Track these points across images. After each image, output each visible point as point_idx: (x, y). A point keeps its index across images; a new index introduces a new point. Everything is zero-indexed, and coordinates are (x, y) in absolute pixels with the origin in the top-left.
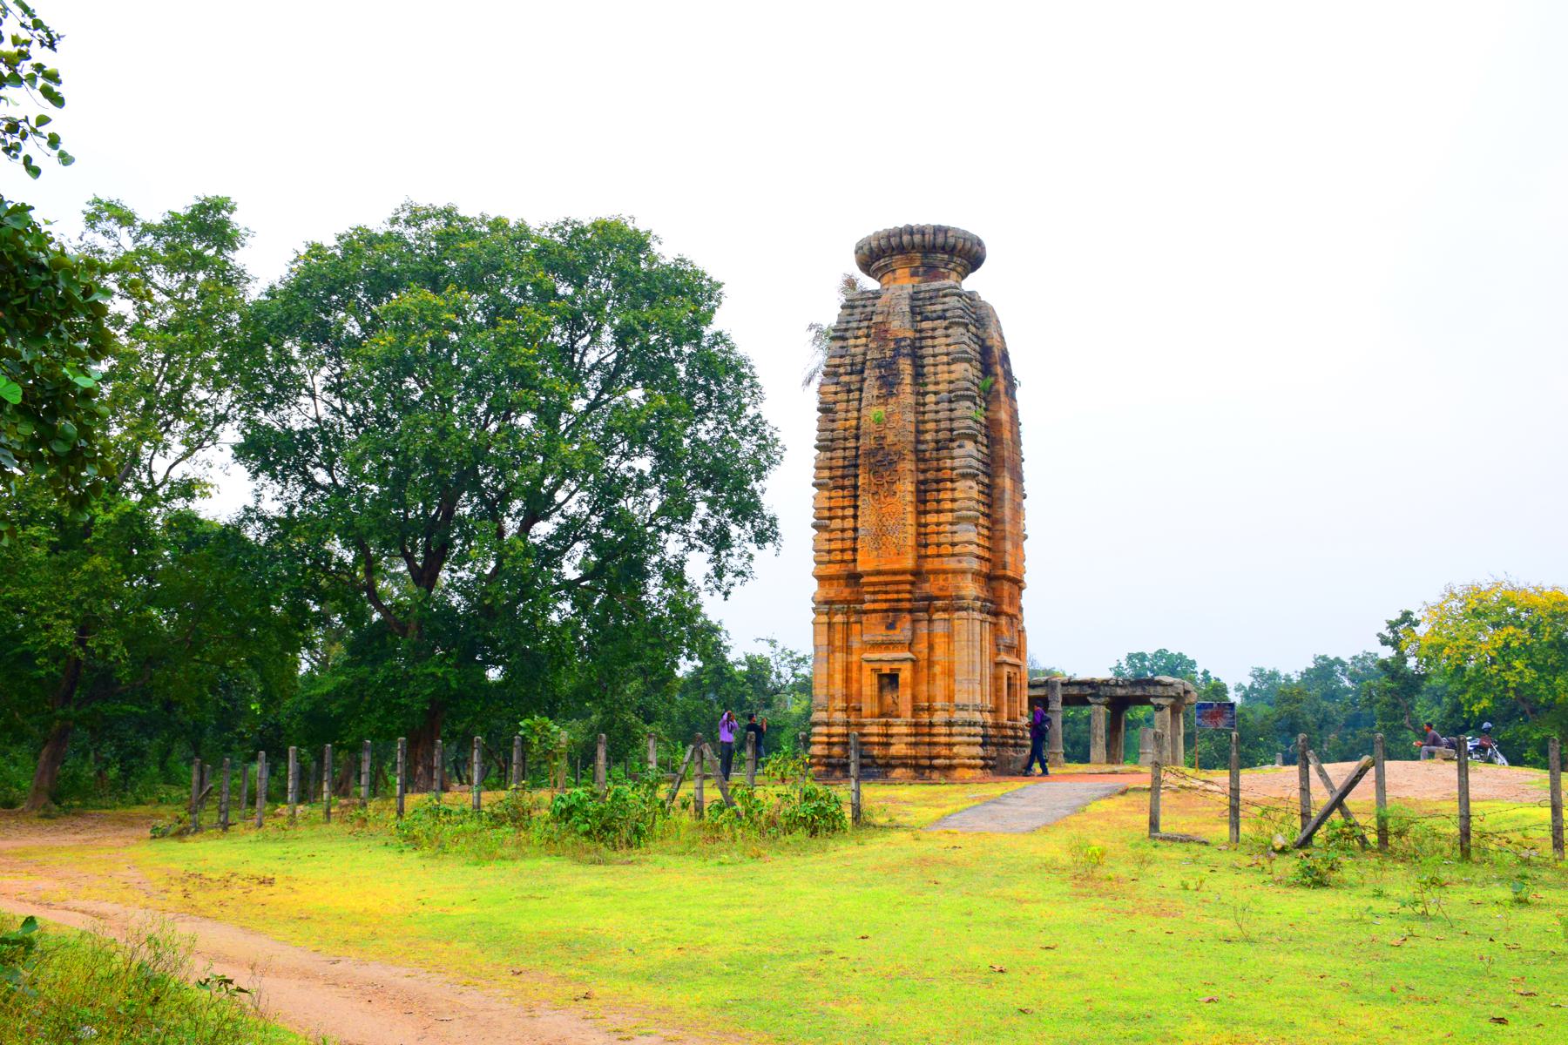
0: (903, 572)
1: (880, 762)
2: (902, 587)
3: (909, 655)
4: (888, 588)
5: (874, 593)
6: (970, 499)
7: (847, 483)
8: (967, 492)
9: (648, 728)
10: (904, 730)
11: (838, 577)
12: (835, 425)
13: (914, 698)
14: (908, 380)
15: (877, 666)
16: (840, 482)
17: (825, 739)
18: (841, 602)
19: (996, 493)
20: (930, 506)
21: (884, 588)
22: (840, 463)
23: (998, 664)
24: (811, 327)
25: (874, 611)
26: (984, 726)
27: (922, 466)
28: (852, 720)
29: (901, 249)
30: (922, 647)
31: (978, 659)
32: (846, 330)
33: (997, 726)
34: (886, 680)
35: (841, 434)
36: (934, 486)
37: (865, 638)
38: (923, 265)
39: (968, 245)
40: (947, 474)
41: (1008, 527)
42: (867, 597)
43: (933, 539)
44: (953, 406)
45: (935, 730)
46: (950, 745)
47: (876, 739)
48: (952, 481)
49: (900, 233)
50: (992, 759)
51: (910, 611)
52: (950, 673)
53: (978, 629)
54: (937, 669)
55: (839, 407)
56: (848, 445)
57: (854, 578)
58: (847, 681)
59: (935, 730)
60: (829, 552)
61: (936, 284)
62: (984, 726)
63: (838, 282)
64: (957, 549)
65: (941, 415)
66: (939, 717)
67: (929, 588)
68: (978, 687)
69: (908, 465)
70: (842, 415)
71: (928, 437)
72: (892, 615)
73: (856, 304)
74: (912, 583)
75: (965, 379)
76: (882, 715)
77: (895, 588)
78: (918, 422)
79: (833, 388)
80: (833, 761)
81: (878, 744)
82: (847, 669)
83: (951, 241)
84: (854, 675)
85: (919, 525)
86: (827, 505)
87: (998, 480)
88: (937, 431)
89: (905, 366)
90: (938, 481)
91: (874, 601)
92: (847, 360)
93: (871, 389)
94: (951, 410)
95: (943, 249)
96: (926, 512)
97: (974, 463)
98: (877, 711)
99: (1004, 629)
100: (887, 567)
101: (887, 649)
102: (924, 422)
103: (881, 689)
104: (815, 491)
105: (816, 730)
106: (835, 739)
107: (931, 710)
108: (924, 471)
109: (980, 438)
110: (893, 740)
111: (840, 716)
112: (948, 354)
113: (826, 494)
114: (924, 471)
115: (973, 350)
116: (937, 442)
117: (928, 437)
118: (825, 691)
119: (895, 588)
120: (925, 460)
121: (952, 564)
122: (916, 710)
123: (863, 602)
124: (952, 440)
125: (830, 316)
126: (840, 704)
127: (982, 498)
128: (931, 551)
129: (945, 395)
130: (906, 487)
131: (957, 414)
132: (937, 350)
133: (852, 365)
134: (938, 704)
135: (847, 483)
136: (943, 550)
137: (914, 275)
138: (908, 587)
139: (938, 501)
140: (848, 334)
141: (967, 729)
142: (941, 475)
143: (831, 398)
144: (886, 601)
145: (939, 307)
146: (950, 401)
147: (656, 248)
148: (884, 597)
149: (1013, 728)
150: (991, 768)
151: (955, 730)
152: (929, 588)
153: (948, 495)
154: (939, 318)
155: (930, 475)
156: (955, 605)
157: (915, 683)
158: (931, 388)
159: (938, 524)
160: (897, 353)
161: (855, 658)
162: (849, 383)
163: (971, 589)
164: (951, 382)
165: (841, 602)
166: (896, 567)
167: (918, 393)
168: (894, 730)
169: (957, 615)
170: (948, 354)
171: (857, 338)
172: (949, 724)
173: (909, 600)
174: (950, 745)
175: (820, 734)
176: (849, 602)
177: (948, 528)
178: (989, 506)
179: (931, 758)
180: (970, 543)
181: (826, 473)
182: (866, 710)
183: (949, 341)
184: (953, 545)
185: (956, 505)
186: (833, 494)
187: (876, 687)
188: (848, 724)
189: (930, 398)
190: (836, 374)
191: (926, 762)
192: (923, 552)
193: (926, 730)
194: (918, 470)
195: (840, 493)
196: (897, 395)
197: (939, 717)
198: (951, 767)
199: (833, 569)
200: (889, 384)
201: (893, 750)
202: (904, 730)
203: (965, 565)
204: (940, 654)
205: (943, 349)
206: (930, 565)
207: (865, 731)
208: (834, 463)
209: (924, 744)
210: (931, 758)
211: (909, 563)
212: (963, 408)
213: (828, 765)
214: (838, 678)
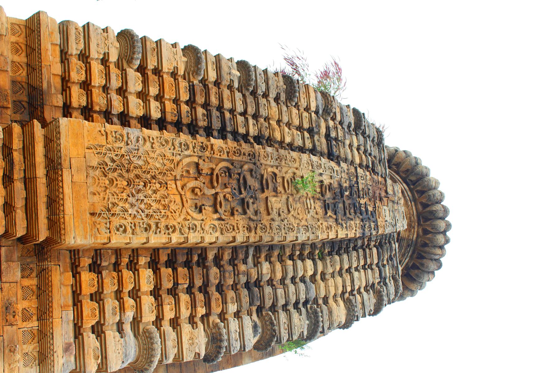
4: (19, 186)
20: (166, 272)
21: (18, 174)
22: (227, 105)
36: (198, 282)
40: (216, 309)
60: (84, 57)
64: (91, 340)
71: (266, 267)
77: (19, 203)
85: (135, 253)
89: (350, 230)
96: (154, 265)
100: (67, 189)
114: (217, 260)
117: (266, 267)
119: (19, 203)
120: (232, 262)
124: (259, 310)
128: (87, 278)
130: (207, 232)
131: (295, 315)
133: (336, 139)
136: (88, 307)
139: (173, 292)
159: (135, 294)
166: (69, 206)
177: (130, 314)
181: (212, 76)
184: (98, 330)
185: (166, 327)
186: (183, 84)
192: (86, 261)
195: (185, 97)
206: (61, 281)
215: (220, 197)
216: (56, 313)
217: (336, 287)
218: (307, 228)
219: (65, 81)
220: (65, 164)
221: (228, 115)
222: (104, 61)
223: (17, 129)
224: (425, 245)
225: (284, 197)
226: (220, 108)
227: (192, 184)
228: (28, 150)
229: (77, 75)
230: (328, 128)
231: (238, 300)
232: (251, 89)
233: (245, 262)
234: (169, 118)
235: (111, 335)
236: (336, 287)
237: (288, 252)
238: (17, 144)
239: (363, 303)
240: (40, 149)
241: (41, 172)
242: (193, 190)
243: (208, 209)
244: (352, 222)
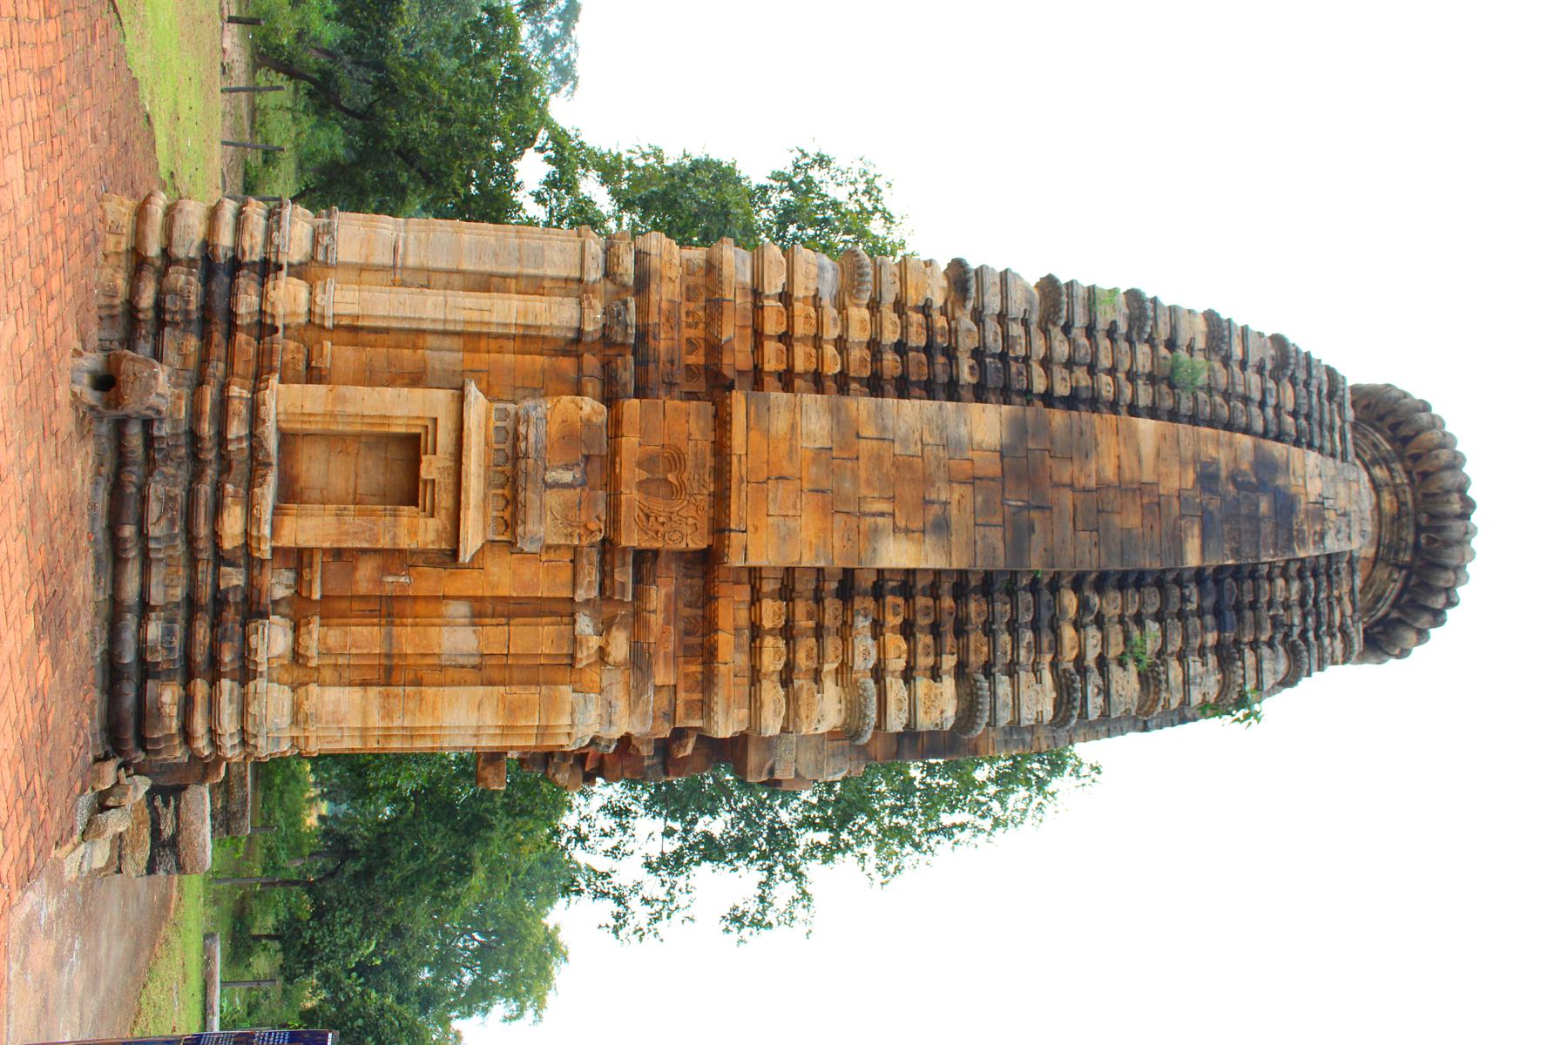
62: (267, 269)
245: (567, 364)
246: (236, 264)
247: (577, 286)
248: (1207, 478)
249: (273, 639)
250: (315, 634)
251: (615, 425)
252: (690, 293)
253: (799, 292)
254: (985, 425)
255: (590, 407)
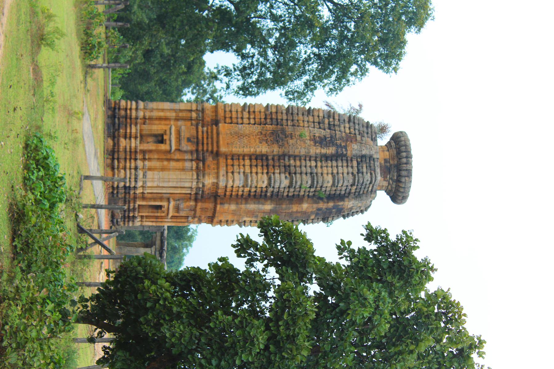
0: (218, 146)
1: (116, 133)
2: (210, 146)
3: (174, 148)
4: (210, 140)
5: (207, 132)
6: (257, 182)
7: (268, 121)
8: (261, 181)
9: (139, 53)
10: (133, 145)
11: (216, 116)
12: (300, 116)
13: (150, 151)
14: (324, 151)
15: (168, 132)
16: (269, 117)
17: (129, 107)
18: (203, 116)
19: (262, 201)
22: (279, 117)
23: (168, 200)
24: (360, 106)
25: (197, 132)
26: (135, 188)
27: (276, 158)
28: (139, 121)
29: (399, 152)
30: (178, 156)
31: (171, 184)
32: (354, 123)
33: (135, 198)
34: (160, 138)
35: (296, 118)
36: (265, 164)
37: (183, 128)
38: (391, 165)
39: (402, 190)
40: (271, 170)
41: (243, 206)
42: (205, 129)
43: (236, 163)
44: (309, 175)
45: (133, 161)
46: (125, 169)
47: (128, 131)
48: (267, 173)
49: (408, 151)
50: (117, 192)
51: (197, 151)
52: (163, 169)
53: (187, 185)
54: (166, 163)
55: (311, 119)
56: (289, 122)
57: (216, 122)
58: (160, 119)
59: (133, 161)
60: (231, 111)
61: (378, 170)
63: (385, 122)
64: (230, 175)
65: (304, 169)
66: (140, 164)
67: (210, 160)
68: (155, 184)
69: (276, 150)
70: (306, 119)
72: (196, 141)
73: (370, 131)
74: (212, 152)
75: (323, 181)
76: (142, 136)
78: (300, 157)
79: (321, 115)
80: (117, 111)
81: (126, 132)
82: (166, 119)
83: (403, 180)
84: (163, 122)
85: (244, 156)
86: (256, 110)
87: (269, 202)
88: (295, 166)
90: (267, 166)
91: (203, 132)
92: (337, 123)
93: (319, 133)
94: (306, 174)
95: (399, 176)
96: (251, 159)
97: (277, 185)
98: (144, 132)
99: (188, 204)
100: (221, 138)
101: (177, 138)
102: (300, 160)
103: (155, 136)
104: (265, 105)
105: (134, 103)
106: (128, 112)
107: (144, 159)
108: (273, 159)
109: (292, 190)
110: (128, 140)
111: (141, 114)
112: (338, 173)
113: (263, 110)
115: (342, 188)
116: (289, 166)
117: (292, 162)
118: (155, 107)
120: (279, 160)
121: (222, 172)
122: (144, 152)
123: (203, 127)
124: (290, 174)
125: (366, 116)
126: (148, 114)
127: (259, 190)
128: (230, 162)
129: (315, 171)
130: (264, 149)
132: (340, 168)
133: (334, 125)
134: (147, 163)
135: (268, 121)
136: (229, 167)
137: (386, 161)
138: (210, 149)
139: (256, 166)
140: (352, 124)
141: (133, 177)
142: (271, 167)
143: (316, 114)
144: (203, 138)
145: (365, 170)
146: (311, 173)
147: (413, 29)
148: (205, 137)
149: (134, 209)
150: (112, 193)
151: (133, 171)
152: (210, 160)
153: (260, 170)
154: (358, 170)
155: (271, 162)
156: (200, 172)
157: (158, 152)
158: (319, 164)
159: (244, 165)
160: (339, 146)
161: (172, 122)
162: (324, 123)
163: (209, 181)
164: (322, 174)
165: (203, 116)
166: (221, 142)
167: (316, 157)
168: (133, 140)
169: (195, 173)
170: (338, 173)
171: (349, 128)
172: (136, 168)
173: (203, 150)
174: (125, 169)
175: (131, 105)
176: (203, 120)
177: (242, 170)
178: (255, 196)
179: (118, 159)
180: (233, 181)
181: (274, 110)
182: (145, 127)
183: (345, 175)
184: (233, 173)
185: (254, 175)
186: (263, 114)
187: (156, 133)
188: (137, 118)
189: (313, 163)
190: (329, 117)
191: (116, 156)
192: (229, 157)
193: (133, 157)
194: (274, 156)
195: (263, 117)
196: (315, 146)
197: (140, 164)
198: (113, 168)
199: (221, 113)
200: (321, 142)
201: (122, 140)
202: (133, 145)
203: (221, 178)
204: (173, 164)
205: (340, 170)
206: (222, 161)
207: (133, 126)
208: (279, 114)
209: (126, 155)
210: (118, 159)
211: (223, 149)
212: (307, 180)
213: (115, 109)
214: (162, 114)
215: (269, 140)
216: (221, 168)
217: (327, 170)
218: (305, 148)
219: (225, 118)
220: (220, 133)
221: (279, 120)
222: (237, 112)
223: (209, 127)
224: (400, 164)
225: (295, 140)
226: (277, 119)
227: (258, 137)
228: (212, 132)
229: (228, 115)
230: (329, 122)
231: (280, 170)
232: (290, 112)
233: (284, 160)
234: (257, 123)
235: (236, 175)
236: (327, 170)
237: (302, 158)
238: (209, 131)
239: (343, 177)
240: (215, 131)
241: (215, 136)
242: (259, 138)
243: (264, 143)
244: (331, 148)
245: (189, 196)
246: (129, 187)
247: (191, 188)
248: (319, 209)
249: (139, 219)
250: (144, 220)
251: (196, 206)
252: (213, 185)
253: (235, 186)
254: (268, 207)
255: (192, 203)
